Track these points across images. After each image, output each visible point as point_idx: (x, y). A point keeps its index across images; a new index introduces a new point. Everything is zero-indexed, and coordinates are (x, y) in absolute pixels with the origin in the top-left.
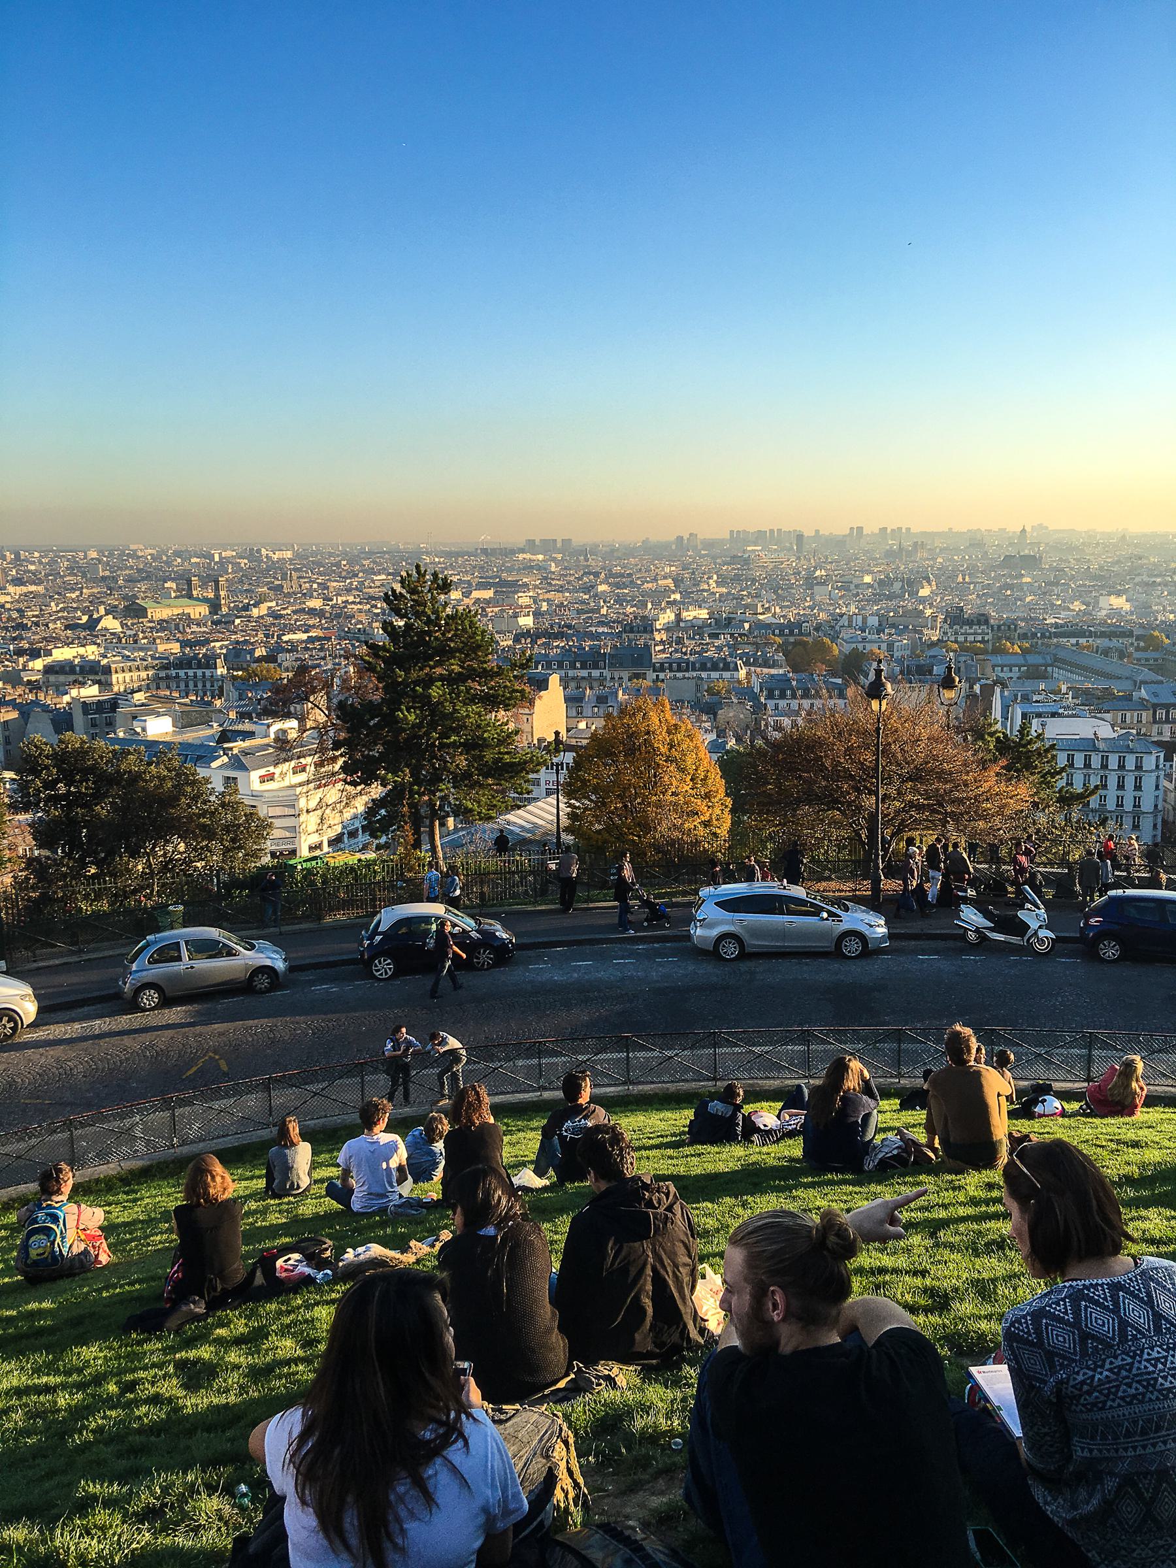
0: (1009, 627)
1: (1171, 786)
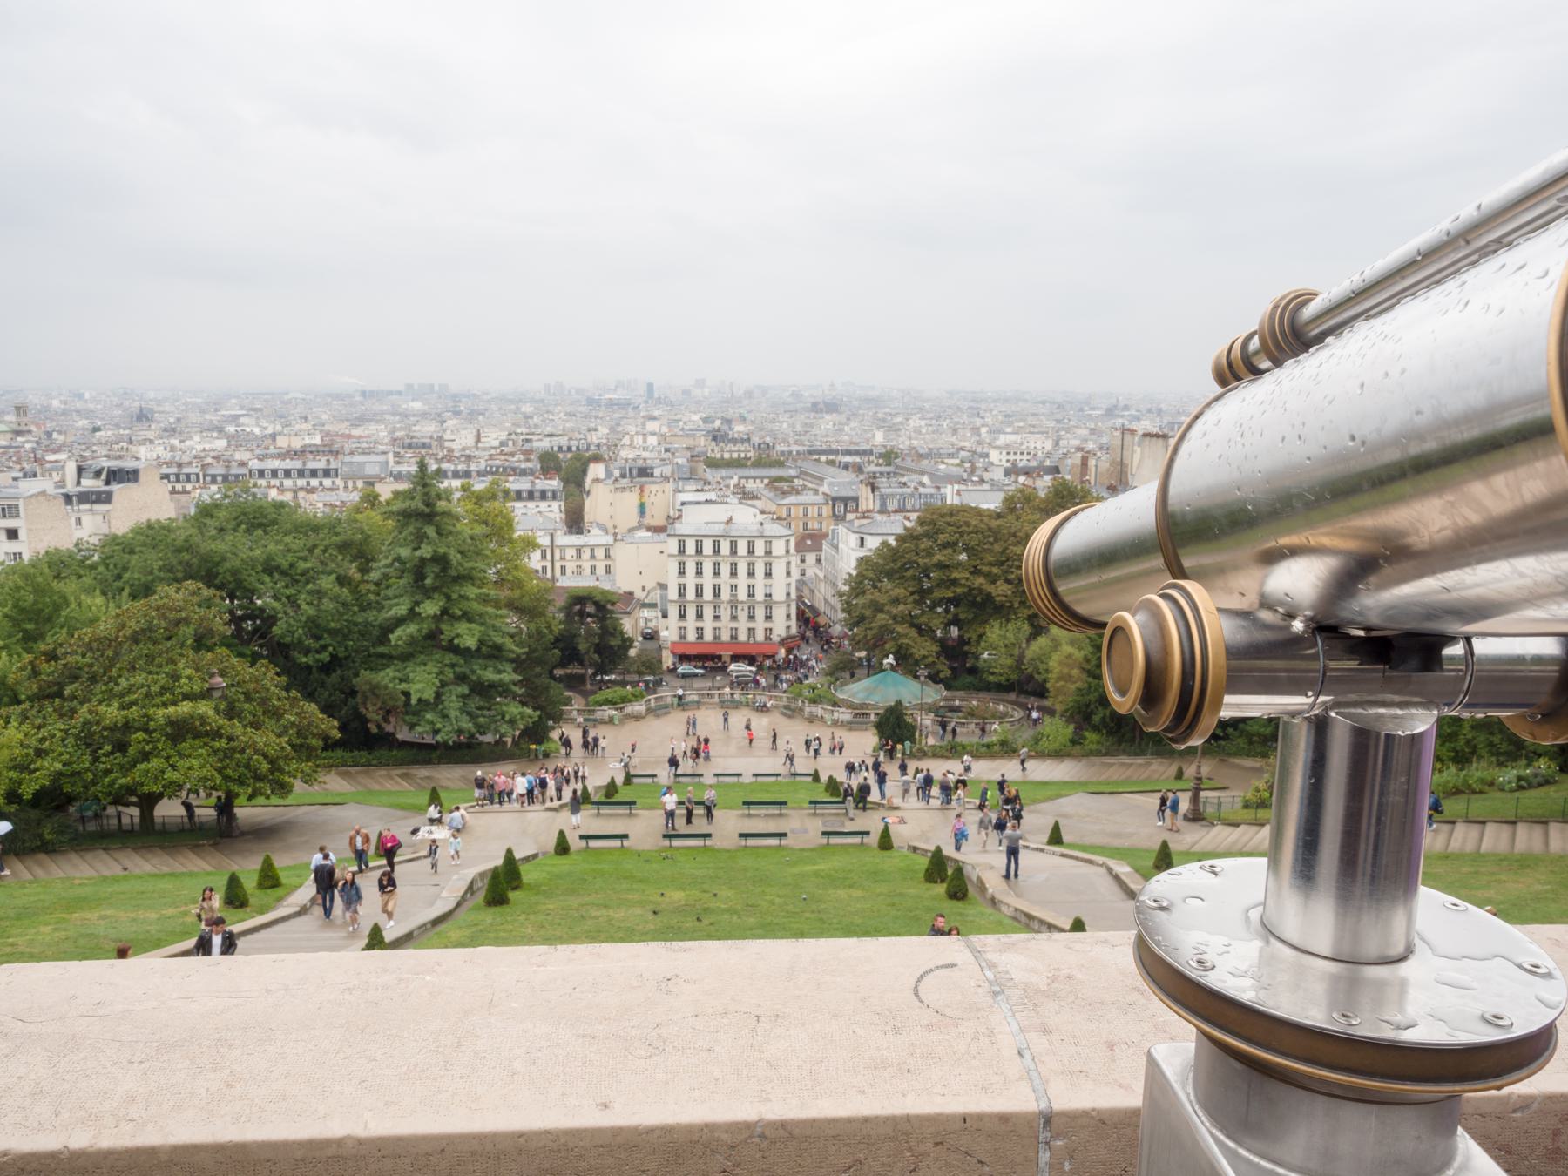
0: (768, 445)
1: (821, 575)
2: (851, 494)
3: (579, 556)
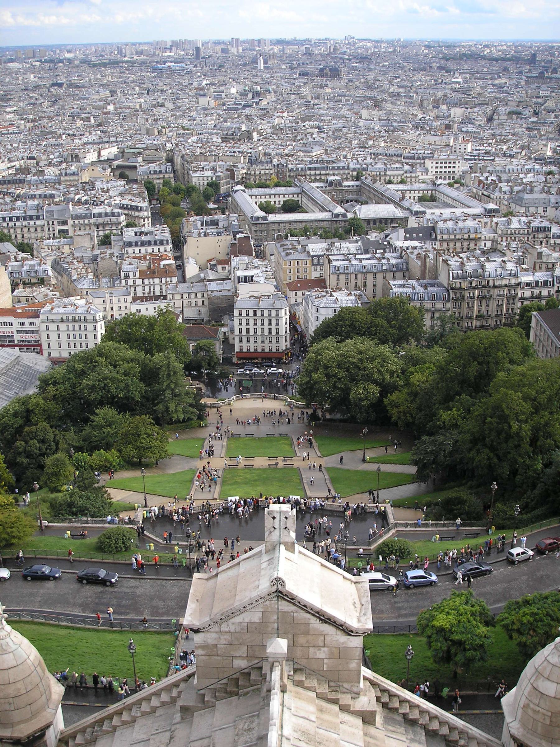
2: (321, 253)
3: (190, 297)
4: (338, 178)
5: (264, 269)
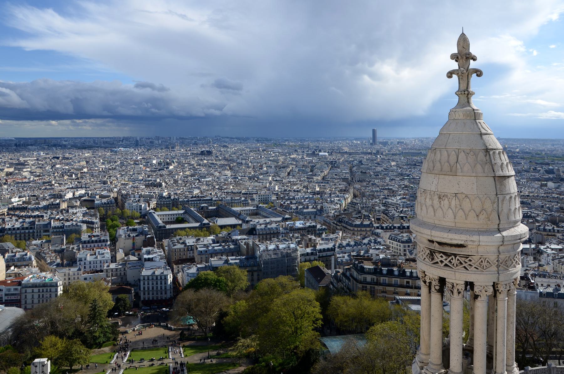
4: (206, 205)
5: (160, 254)
